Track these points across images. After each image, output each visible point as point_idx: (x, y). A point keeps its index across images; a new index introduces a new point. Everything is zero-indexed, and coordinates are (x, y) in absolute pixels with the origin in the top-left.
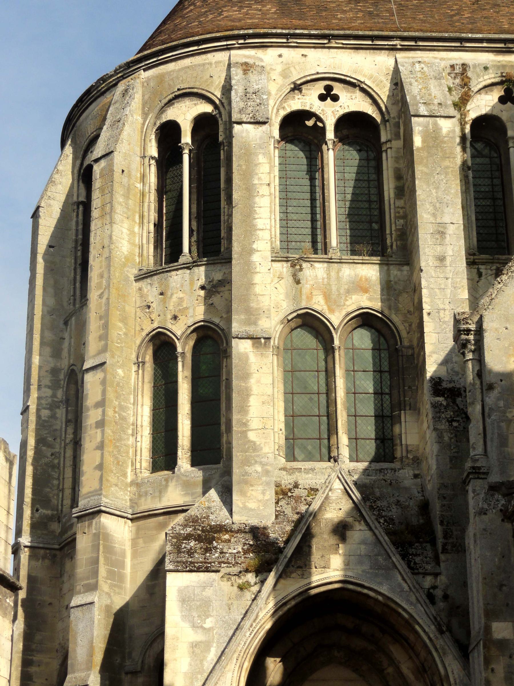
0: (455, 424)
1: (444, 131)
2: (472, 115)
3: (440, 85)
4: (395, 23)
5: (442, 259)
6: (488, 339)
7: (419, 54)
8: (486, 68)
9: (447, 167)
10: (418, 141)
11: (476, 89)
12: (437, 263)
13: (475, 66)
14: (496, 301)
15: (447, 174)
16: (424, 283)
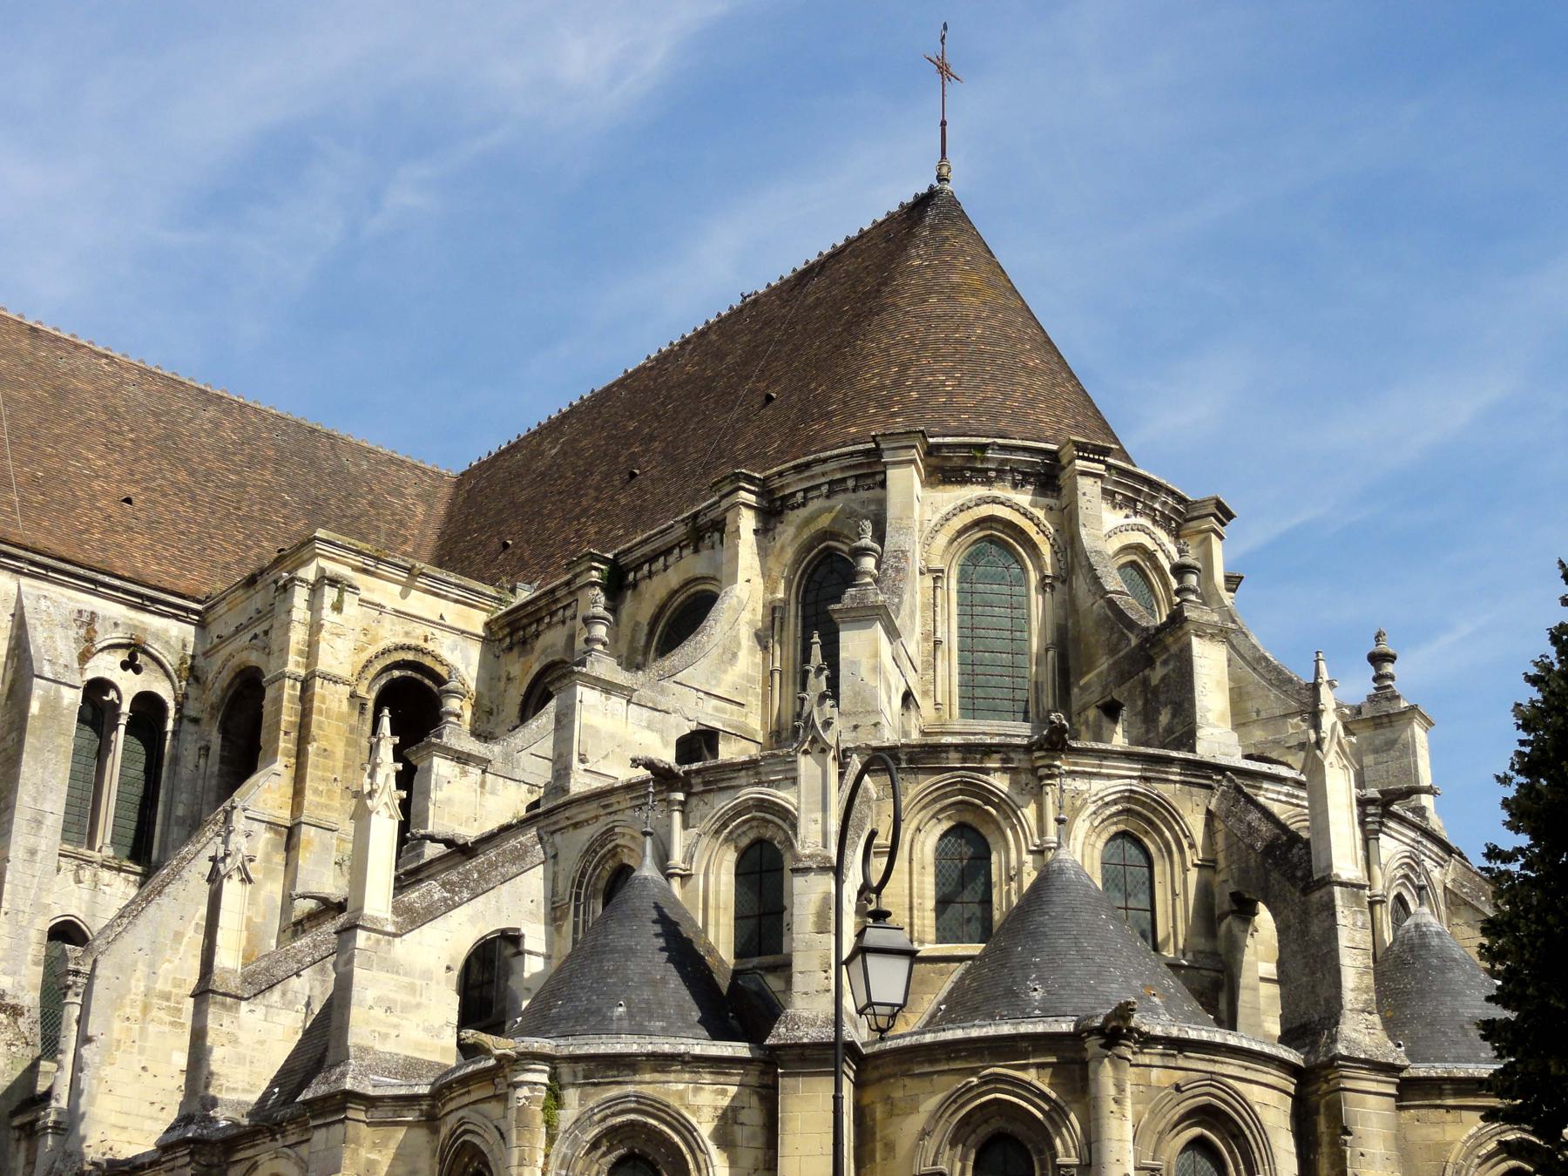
0: (13, 1049)
1: (66, 702)
2: (89, 675)
3: (67, 637)
4: (17, 527)
5: (33, 852)
6: (98, 986)
7: (45, 585)
8: (116, 624)
9: (60, 746)
10: (35, 707)
11: (99, 646)
12: (26, 857)
13: (104, 618)
14: (113, 947)
15: (58, 753)
16: (8, 877)
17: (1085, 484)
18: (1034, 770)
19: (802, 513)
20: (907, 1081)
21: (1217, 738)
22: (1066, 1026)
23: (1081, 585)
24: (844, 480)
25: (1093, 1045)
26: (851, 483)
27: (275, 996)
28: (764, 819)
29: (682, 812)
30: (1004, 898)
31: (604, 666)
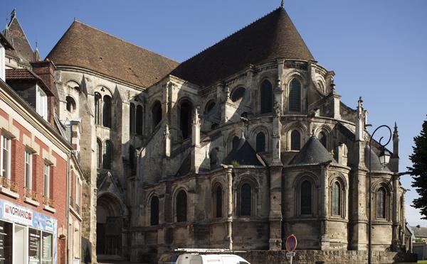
17: (313, 68)
21: (337, 116)
22: (317, 164)
23: (311, 87)
25: (322, 167)
27: (176, 158)
30: (302, 144)
31: (229, 101)
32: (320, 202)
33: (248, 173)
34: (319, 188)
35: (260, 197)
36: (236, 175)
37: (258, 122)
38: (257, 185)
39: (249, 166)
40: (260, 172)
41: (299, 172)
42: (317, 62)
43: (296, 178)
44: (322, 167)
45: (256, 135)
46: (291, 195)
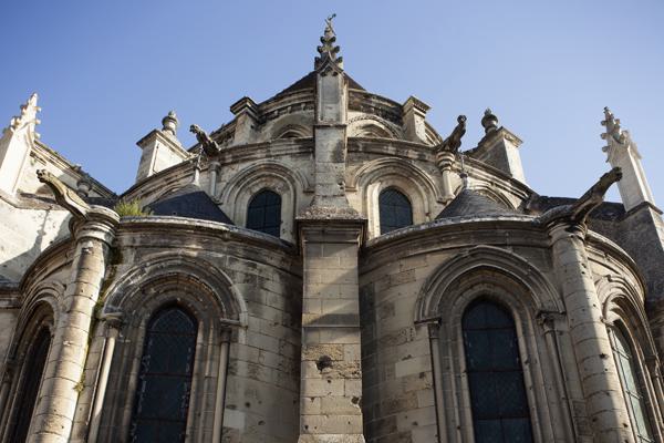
18: (437, 164)
19: (276, 120)
20: (403, 262)
24: (300, 104)
25: (558, 231)
26: (303, 106)
28: (270, 175)
29: (218, 173)
32: (576, 393)
33: (193, 249)
34: (560, 326)
35: (242, 368)
36: (129, 256)
37: (259, 154)
38: (233, 310)
39: (196, 222)
40: (252, 259)
41: (439, 259)
42: (428, 108)
43: (432, 280)
44: (558, 231)
45: (247, 198)
46: (412, 362)
